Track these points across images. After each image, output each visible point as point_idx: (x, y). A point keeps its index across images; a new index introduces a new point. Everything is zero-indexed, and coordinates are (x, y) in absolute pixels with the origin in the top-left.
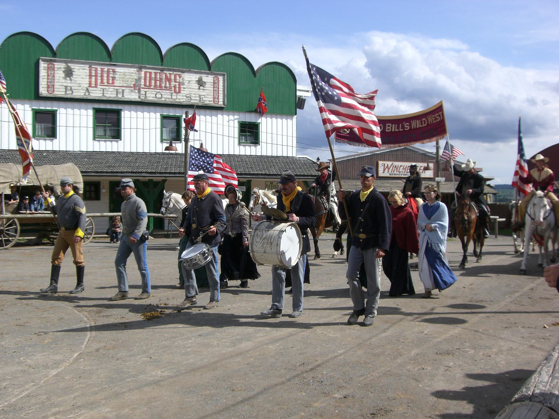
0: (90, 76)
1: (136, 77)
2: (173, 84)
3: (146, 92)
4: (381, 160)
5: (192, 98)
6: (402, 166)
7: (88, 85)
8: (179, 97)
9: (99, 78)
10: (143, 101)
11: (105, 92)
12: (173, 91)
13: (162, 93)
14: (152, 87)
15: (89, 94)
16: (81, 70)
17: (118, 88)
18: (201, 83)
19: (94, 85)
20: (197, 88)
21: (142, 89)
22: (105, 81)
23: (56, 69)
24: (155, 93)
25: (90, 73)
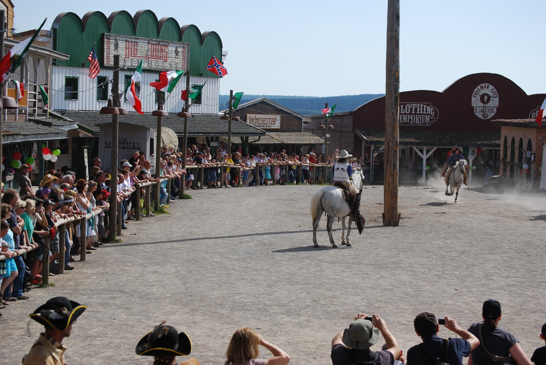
0: (126, 48)
1: (147, 49)
2: (164, 53)
3: (151, 61)
4: (250, 113)
5: (173, 66)
6: (260, 118)
7: (125, 56)
8: (167, 65)
9: (130, 50)
10: (151, 69)
11: (133, 62)
12: (164, 60)
13: (159, 62)
14: (154, 57)
15: (125, 64)
16: (122, 44)
17: (139, 58)
18: (177, 53)
19: (127, 56)
20: (175, 57)
21: (149, 59)
22: (133, 52)
23: (111, 43)
24: (155, 62)
25: (126, 45)
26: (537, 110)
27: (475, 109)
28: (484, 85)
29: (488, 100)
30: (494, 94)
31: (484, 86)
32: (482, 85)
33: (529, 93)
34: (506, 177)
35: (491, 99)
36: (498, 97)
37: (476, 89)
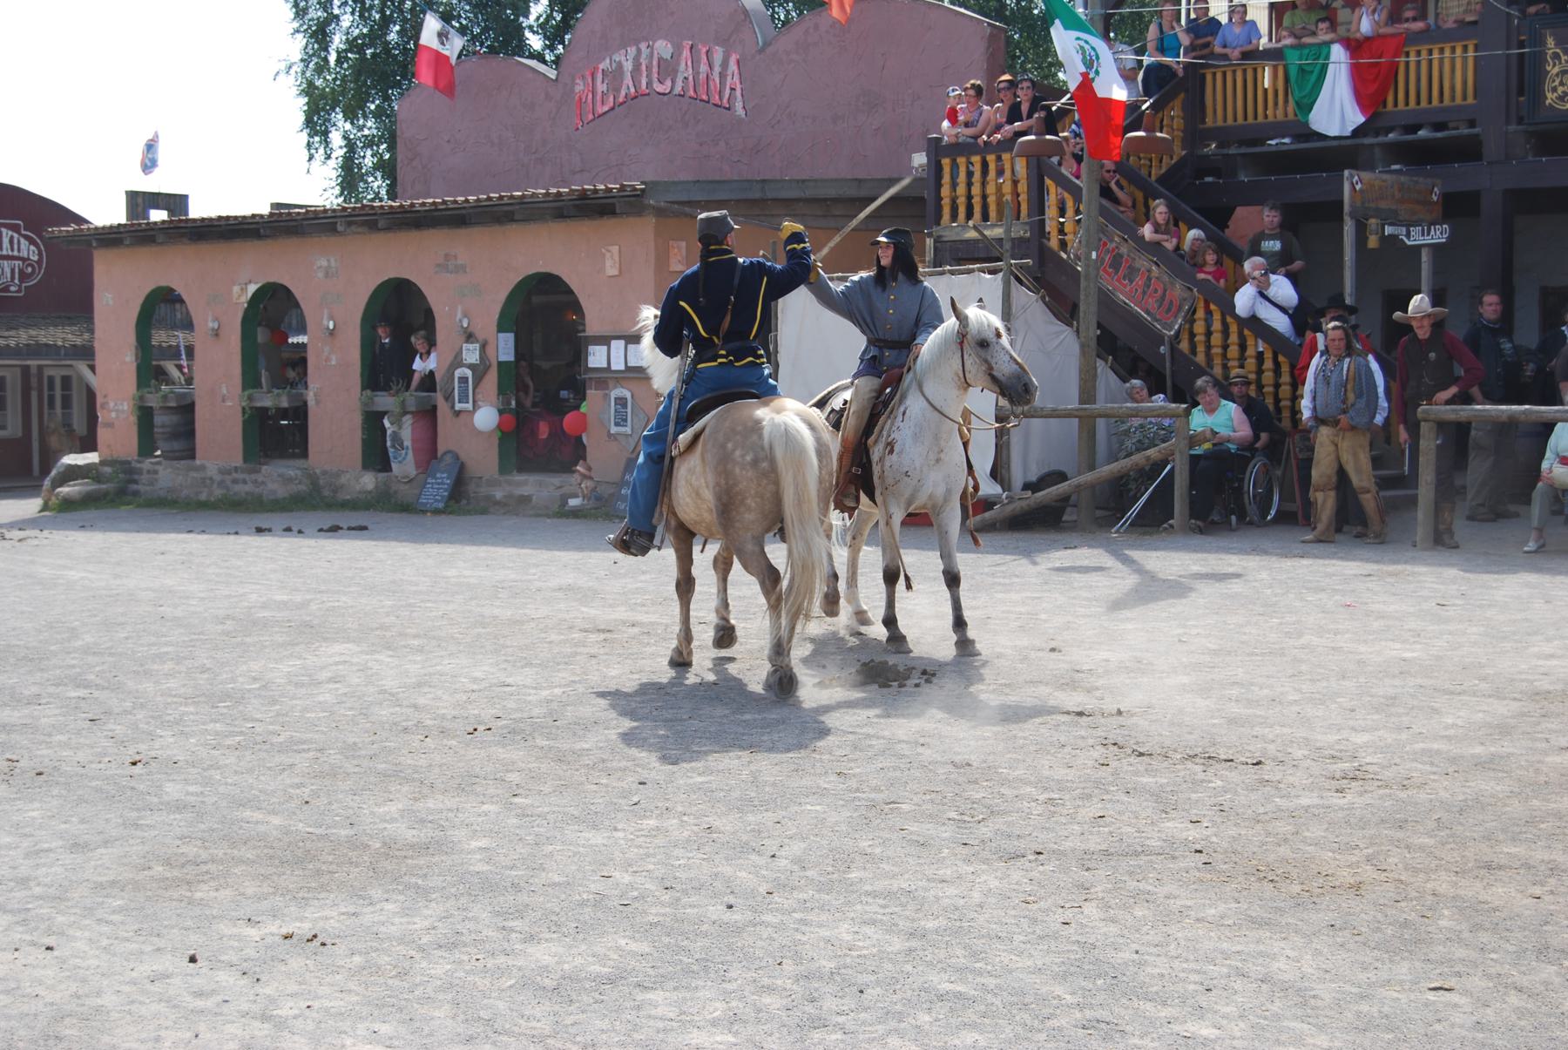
34: (193, 457)
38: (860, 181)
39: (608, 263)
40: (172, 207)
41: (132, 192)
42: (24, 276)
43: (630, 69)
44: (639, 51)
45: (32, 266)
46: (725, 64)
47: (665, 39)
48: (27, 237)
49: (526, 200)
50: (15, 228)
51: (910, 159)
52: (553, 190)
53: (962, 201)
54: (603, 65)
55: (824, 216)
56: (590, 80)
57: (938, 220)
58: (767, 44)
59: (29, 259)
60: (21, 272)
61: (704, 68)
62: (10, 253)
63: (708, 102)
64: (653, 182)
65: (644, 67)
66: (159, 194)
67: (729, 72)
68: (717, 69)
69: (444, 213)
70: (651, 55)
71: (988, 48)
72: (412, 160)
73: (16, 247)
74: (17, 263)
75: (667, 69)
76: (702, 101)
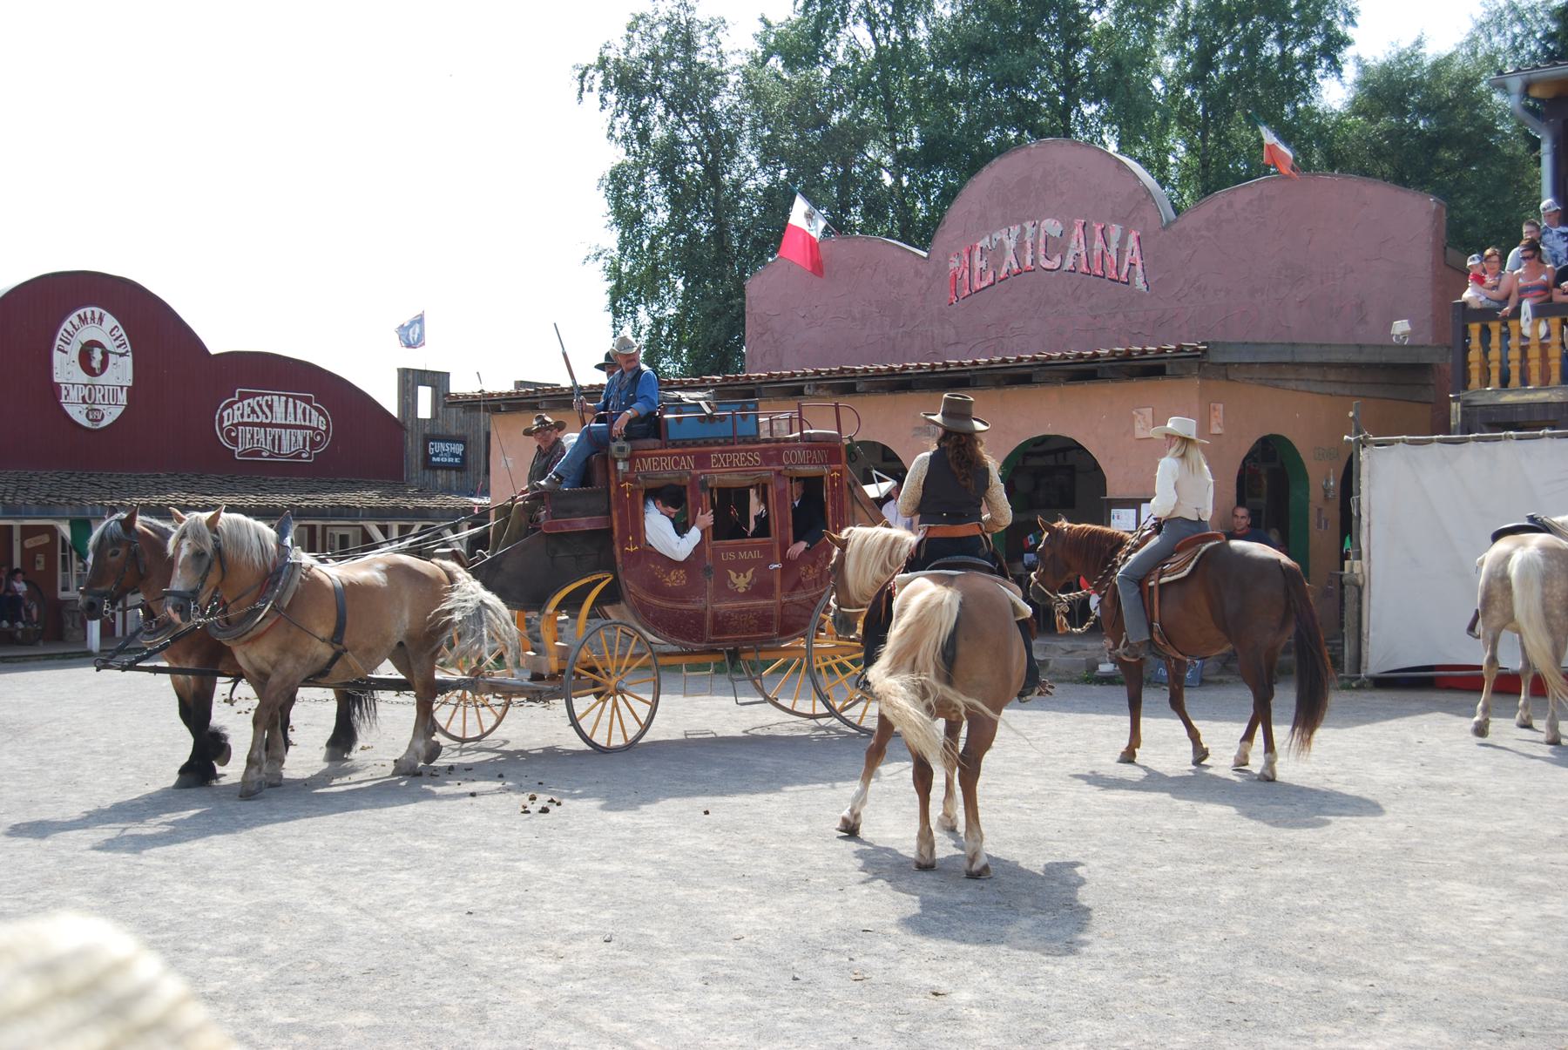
26: (235, 402)
27: (64, 393)
28: (88, 310)
29: (104, 364)
30: (119, 346)
31: (89, 315)
32: (85, 313)
33: (215, 346)
35: (112, 358)
36: (130, 354)
37: (66, 325)
38: (1360, 346)
39: (1213, 423)
40: (436, 383)
41: (404, 369)
42: (314, 444)
43: (1013, 246)
44: (1023, 230)
45: (321, 435)
46: (1123, 241)
47: (1053, 217)
48: (316, 408)
49: (937, 370)
50: (308, 401)
51: (1390, 325)
52: (982, 360)
53: (1495, 367)
54: (985, 242)
55: (1322, 381)
56: (966, 258)
57: (1465, 382)
58: (1169, 223)
59: (318, 429)
60: (311, 439)
61: (1098, 245)
62: (303, 423)
63: (1104, 277)
64: (1213, 343)
65: (1029, 245)
66: (426, 371)
67: (1129, 248)
68: (1114, 246)
69: (942, 376)
70: (1038, 233)
71: (1434, 222)
72: (762, 334)
73: (308, 417)
74: (308, 432)
75: (1055, 246)
76: (1095, 276)
